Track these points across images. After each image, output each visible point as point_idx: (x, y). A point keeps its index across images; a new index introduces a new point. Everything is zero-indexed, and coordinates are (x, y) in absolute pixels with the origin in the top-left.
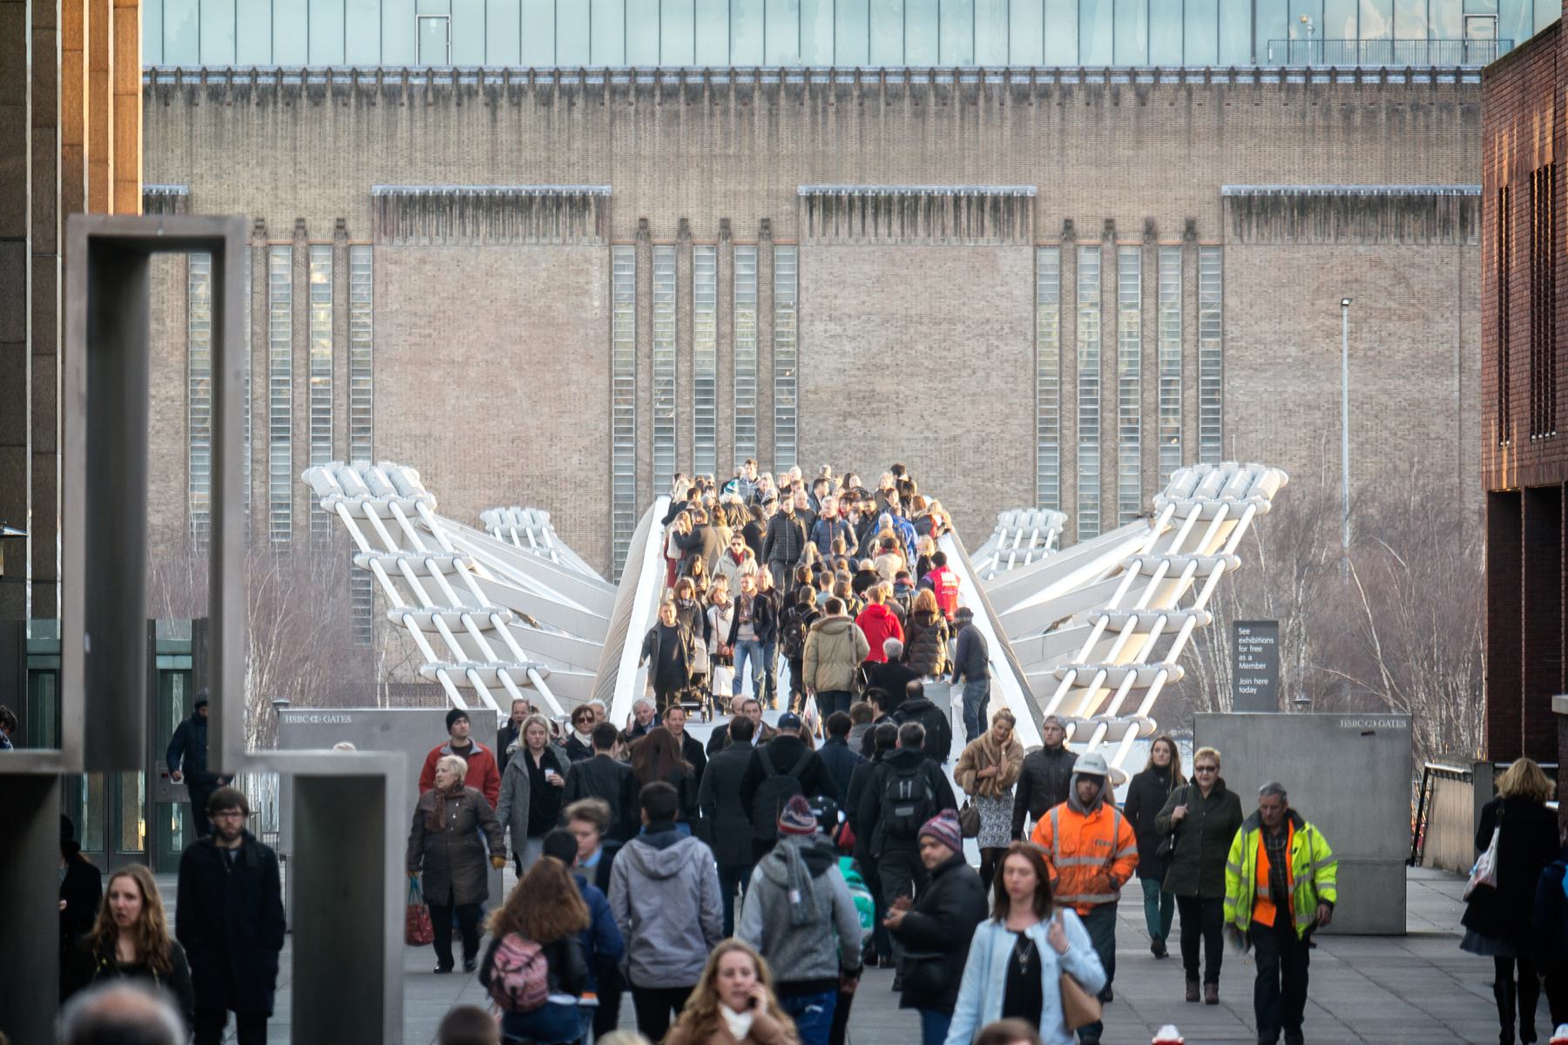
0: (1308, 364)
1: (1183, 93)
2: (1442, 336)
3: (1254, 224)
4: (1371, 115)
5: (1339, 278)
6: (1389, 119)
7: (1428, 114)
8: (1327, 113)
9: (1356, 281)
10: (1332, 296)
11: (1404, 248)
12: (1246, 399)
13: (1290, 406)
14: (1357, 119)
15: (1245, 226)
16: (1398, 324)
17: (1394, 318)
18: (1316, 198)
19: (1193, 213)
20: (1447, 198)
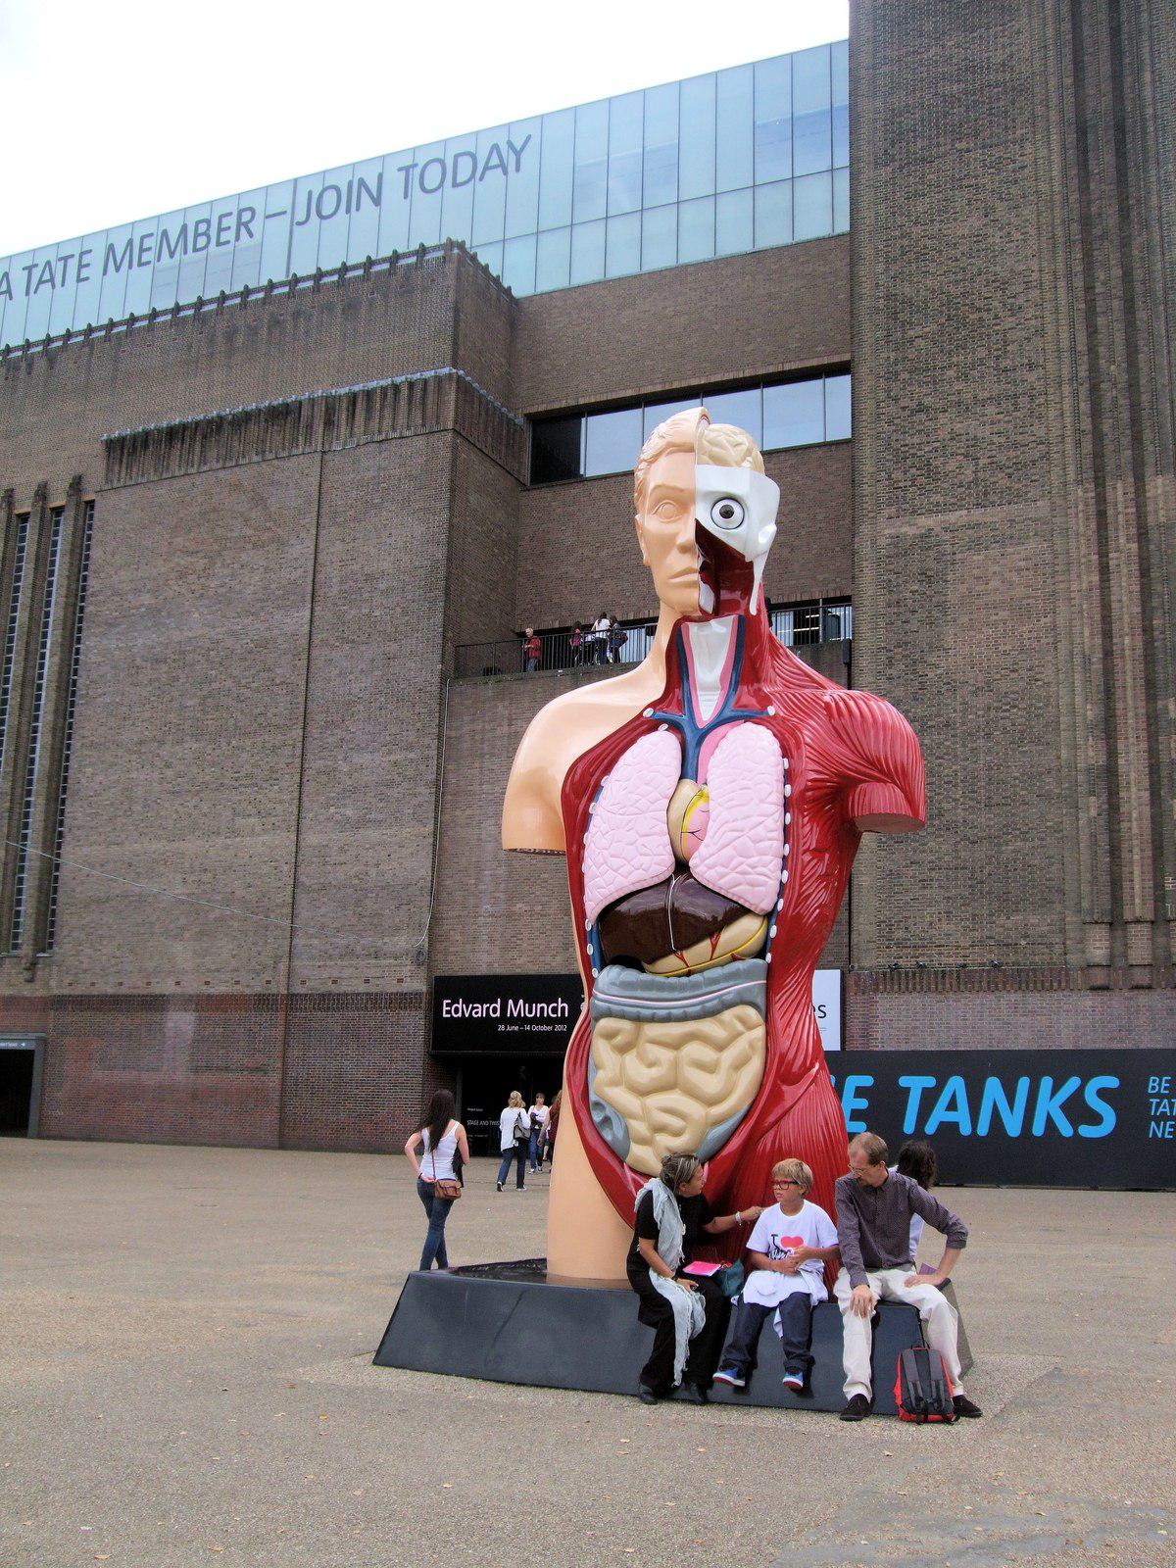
0: (160, 611)
1: (87, 349)
2: (296, 559)
3: (124, 465)
4: (253, 331)
5: (197, 510)
6: (270, 333)
7: (309, 318)
8: (211, 341)
9: (215, 510)
10: (190, 531)
11: (264, 465)
12: (100, 659)
13: (139, 662)
14: (240, 339)
15: (116, 468)
16: (251, 553)
17: (249, 546)
18: (184, 427)
19: (80, 470)
20: (312, 401)
